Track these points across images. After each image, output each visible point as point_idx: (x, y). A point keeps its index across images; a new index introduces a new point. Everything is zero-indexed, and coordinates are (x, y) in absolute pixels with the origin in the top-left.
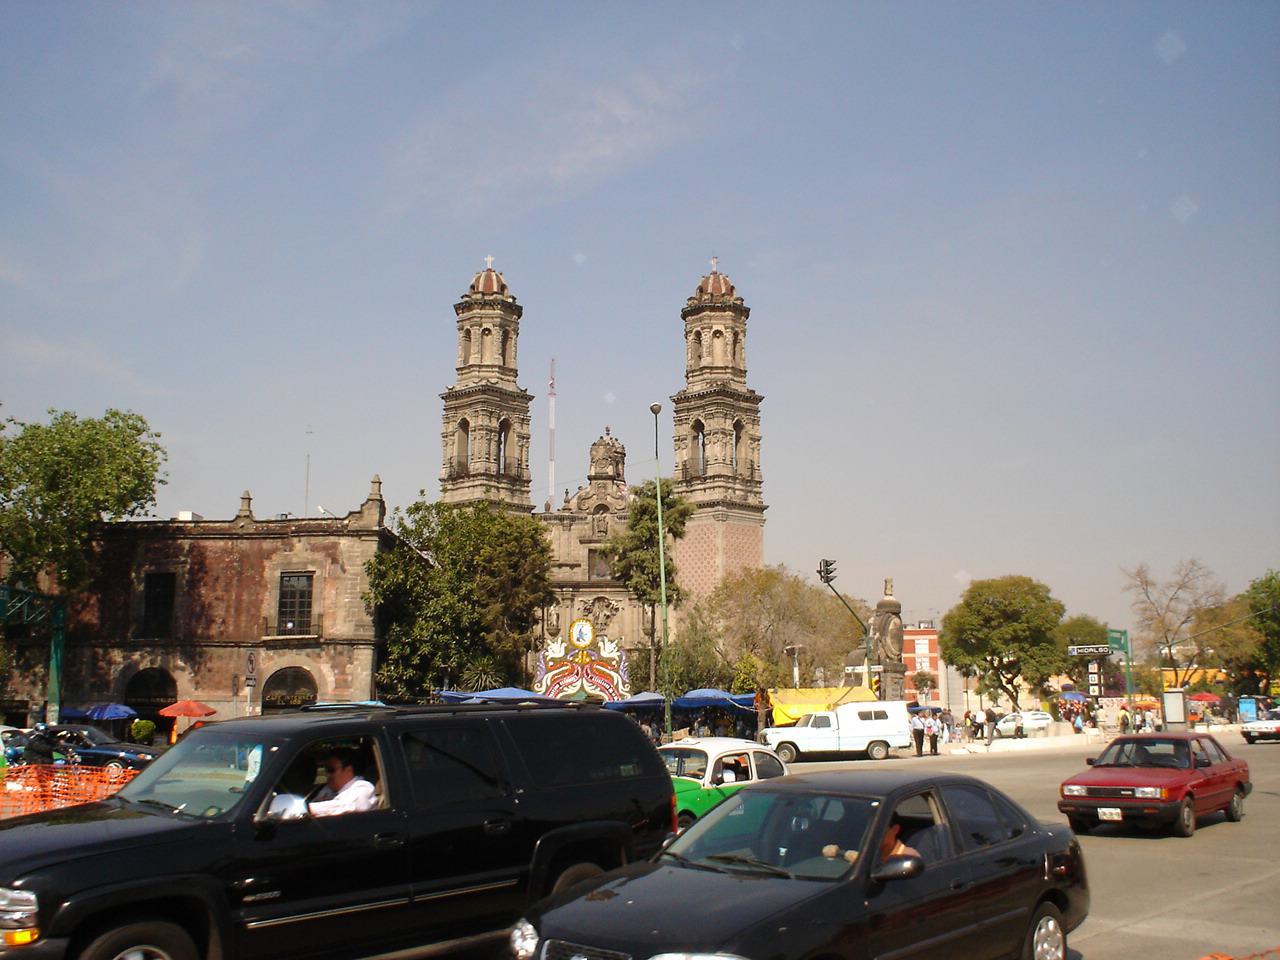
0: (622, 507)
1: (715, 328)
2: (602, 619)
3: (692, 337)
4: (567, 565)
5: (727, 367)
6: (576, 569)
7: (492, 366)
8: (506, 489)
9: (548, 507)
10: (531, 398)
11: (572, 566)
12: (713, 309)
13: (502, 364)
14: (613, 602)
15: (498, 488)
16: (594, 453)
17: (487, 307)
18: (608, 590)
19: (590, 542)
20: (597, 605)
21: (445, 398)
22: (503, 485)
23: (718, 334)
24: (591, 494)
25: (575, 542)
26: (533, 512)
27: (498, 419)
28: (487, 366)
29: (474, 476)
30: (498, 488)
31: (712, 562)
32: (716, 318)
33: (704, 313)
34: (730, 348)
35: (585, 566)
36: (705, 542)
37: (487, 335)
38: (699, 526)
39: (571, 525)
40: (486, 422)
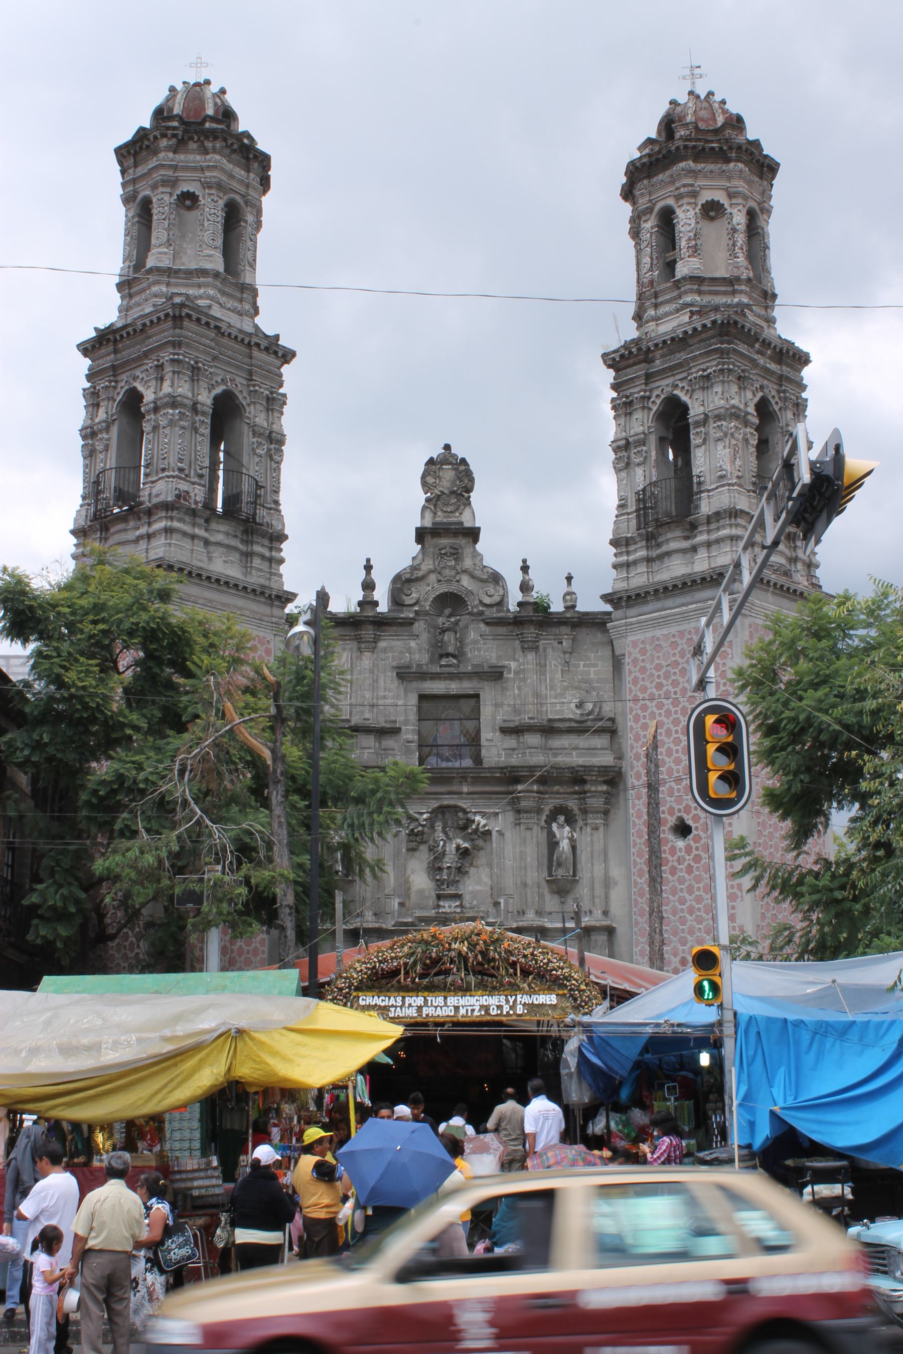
0: (496, 599)
1: (706, 196)
2: (450, 860)
3: (649, 225)
4: (367, 730)
5: (738, 279)
6: (389, 742)
7: (203, 272)
8: (228, 547)
9: (323, 597)
10: (287, 356)
11: (382, 733)
12: (699, 155)
13: (221, 268)
14: (478, 818)
15: (207, 543)
16: (430, 480)
17: (192, 145)
18: (465, 789)
19: (423, 676)
20: (439, 826)
21: (87, 349)
22: (220, 537)
23: (712, 211)
24: (425, 568)
25: (388, 682)
27: (210, 391)
28: (189, 273)
29: (149, 513)
30: (207, 543)
32: (710, 175)
33: (682, 165)
34: (741, 239)
35: (409, 733)
37: (189, 208)
38: (681, 633)
39: (376, 640)
40: (184, 389)
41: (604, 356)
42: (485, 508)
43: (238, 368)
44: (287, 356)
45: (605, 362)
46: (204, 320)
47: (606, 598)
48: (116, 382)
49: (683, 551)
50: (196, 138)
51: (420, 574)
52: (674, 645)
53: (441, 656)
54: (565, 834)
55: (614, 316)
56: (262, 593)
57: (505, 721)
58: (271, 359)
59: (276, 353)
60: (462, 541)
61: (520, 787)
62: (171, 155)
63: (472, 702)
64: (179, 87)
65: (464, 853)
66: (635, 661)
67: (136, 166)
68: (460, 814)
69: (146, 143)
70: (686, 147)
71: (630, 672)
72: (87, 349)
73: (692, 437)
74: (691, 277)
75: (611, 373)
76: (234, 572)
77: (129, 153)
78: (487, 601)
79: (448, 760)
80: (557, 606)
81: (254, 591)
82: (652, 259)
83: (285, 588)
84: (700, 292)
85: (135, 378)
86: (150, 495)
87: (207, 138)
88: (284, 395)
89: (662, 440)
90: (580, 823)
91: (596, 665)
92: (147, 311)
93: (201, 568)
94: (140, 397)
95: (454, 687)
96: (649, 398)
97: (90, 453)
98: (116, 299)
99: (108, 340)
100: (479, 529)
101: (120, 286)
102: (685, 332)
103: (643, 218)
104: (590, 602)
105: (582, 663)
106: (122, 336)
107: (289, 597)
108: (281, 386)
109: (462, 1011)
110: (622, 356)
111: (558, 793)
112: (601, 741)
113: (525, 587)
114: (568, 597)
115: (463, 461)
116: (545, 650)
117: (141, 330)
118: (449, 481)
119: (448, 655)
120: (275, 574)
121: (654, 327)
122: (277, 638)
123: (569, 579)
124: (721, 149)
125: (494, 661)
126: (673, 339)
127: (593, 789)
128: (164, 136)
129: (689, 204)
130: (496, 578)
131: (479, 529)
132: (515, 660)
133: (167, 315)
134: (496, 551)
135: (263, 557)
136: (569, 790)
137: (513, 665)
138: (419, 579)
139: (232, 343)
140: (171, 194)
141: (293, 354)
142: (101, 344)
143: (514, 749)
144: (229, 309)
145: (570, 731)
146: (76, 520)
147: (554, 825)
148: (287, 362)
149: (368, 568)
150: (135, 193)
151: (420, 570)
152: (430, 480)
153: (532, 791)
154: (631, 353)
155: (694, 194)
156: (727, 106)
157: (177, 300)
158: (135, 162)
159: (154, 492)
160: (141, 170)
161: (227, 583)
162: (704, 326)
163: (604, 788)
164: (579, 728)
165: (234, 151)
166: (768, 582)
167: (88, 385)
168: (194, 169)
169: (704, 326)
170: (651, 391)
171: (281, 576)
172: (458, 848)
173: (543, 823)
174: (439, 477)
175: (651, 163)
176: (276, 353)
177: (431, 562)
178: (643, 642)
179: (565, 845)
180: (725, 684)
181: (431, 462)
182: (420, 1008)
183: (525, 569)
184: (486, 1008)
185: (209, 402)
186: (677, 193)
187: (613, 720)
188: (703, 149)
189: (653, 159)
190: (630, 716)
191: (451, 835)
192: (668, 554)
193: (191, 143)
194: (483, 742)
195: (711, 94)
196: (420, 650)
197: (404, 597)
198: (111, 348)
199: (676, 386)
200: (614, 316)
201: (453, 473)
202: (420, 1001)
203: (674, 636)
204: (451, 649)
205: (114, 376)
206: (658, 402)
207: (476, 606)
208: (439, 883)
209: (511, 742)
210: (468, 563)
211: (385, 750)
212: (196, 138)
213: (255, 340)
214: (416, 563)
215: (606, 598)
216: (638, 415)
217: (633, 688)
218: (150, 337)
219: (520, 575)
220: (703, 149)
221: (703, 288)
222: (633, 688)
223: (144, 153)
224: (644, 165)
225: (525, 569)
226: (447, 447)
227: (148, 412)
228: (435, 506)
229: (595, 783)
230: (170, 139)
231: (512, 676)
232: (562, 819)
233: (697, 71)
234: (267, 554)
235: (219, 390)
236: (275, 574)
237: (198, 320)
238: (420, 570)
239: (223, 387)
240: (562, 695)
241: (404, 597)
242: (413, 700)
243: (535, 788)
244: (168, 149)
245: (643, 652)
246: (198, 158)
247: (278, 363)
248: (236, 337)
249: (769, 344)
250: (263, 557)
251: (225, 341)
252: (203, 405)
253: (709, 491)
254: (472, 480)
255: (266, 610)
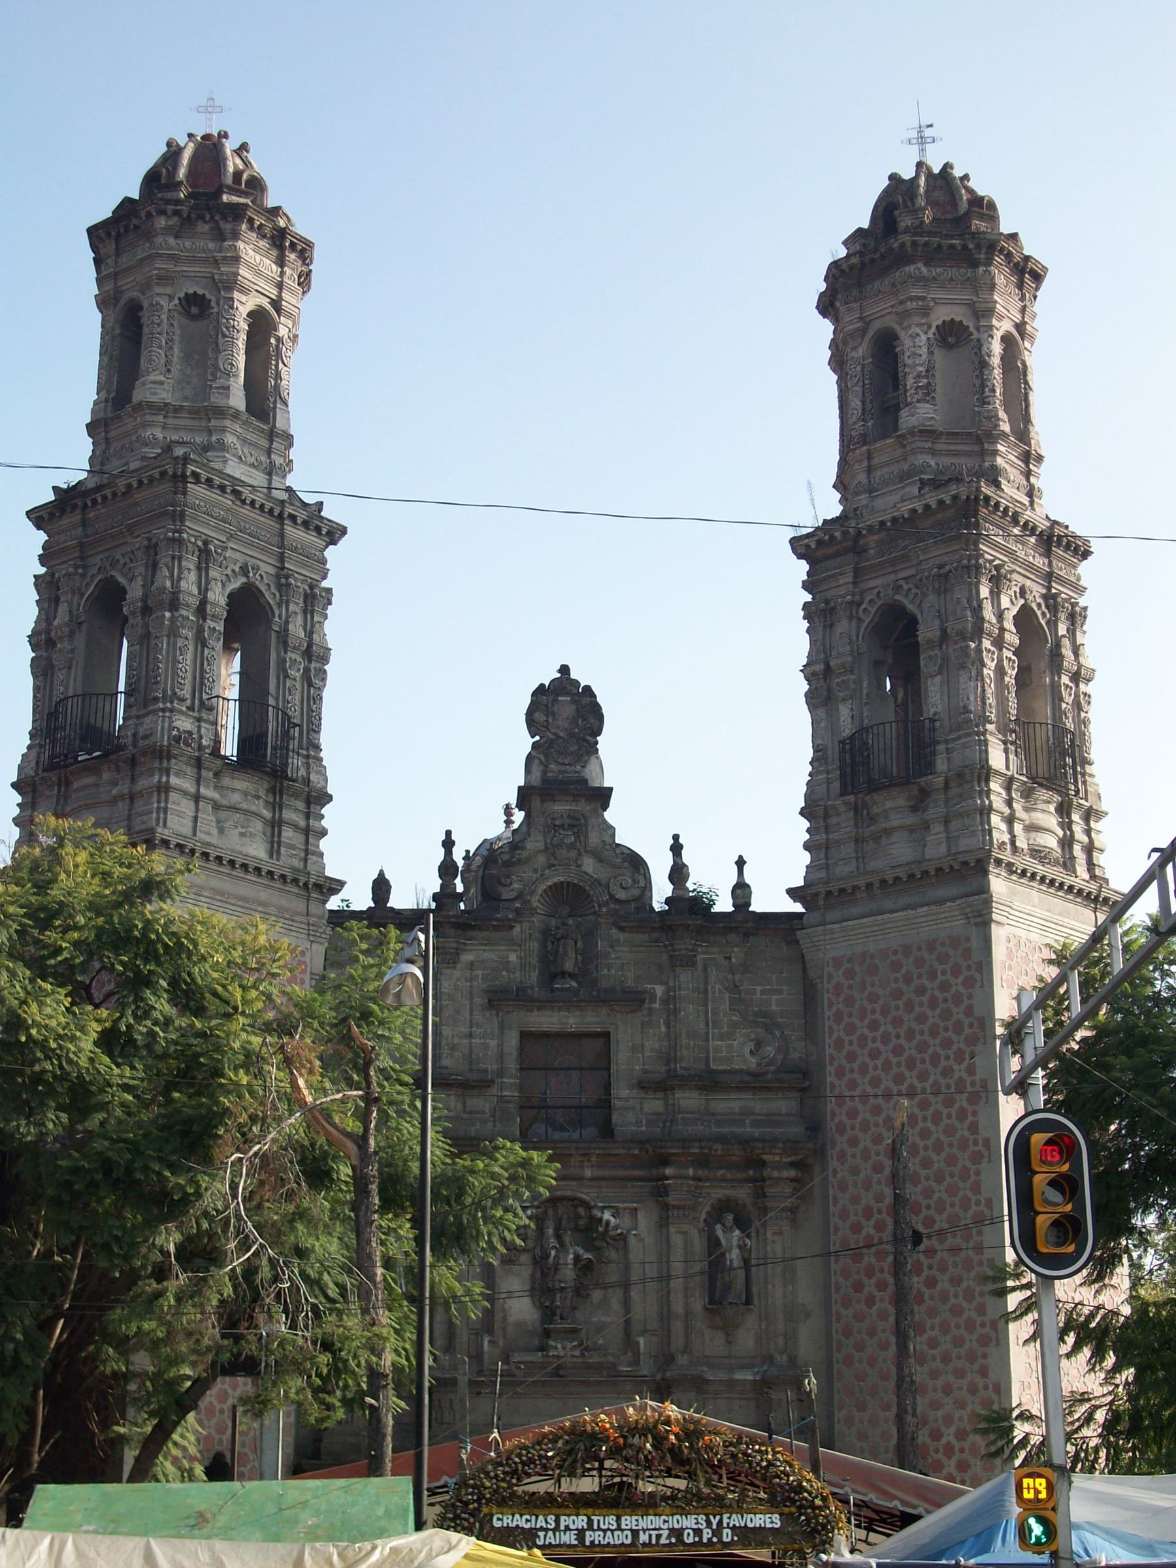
1: (942, 315)
3: (861, 352)
9: (381, 887)
10: (335, 533)
16: (539, 717)
21: (39, 517)
26: (334, 903)
27: (224, 586)
31: (959, 1071)
36: (933, 1003)
38: (907, 950)
41: (794, 542)
42: (617, 758)
43: (263, 550)
44: (335, 533)
45: (794, 551)
46: (217, 481)
47: (793, 893)
48: (85, 567)
49: (911, 830)
50: (208, 217)
51: (525, 854)
52: (896, 966)
53: (554, 977)
54: (735, 1242)
55: (809, 483)
56: (295, 881)
57: (647, 1072)
58: (310, 538)
59: (318, 529)
60: (583, 807)
61: (668, 1171)
62: (171, 241)
63: (600, 1042)
64: (182, 140)
65: (584, 1268)
66: (838, 989)
67: (118, 253)
68: (581, 1211)
69: (135, 221)
70: (914, 243)
71: (831, 1004)
72: (39, 517)
73: (922, 663)
74: (921, 431)
75: (803, 567)
76: (257, 850)
77: (109, 235)
78: (622, 895)
79: (562, 1129)
80: (724, 904)
81: (283, 877)
82: (863, 402)
83: (329, 873)
84: (932, 452)
85: (114, 563)
86: (135, 735)
87: (224, 218)
88: (329, 591)
89: (877, 664)
90: (757, 1224)
91: (779, 992)
92: (133, 466)
93: (208, 844)
94: (121, 592)
95: (572, 1021)
96: (859, 604)
97: (42, 670)
98: (86, 446)
99: (75, 506)
100: (611, 789)
101: (91, 428)
102: (914, 511)
103: (851, 344)
104: (772, 898)
105: (759, 988)
106: (95, 502)
107: (335, 886)
108: (324, 577)
109: (644, 1538)
110: (820, 543)
111: (724, 1180)
112: (784, 1105)
113: (678, 873)
114: (738, 891)
115: (588, 689)
116: (705, 969)
117: (124, 494)
118: (565, 718)
119: (563, 974)
120: (314, 853)
121: (865, 502)
122: (315, 946)
123: (741, 863)
124: (965, 247)
125: (630, 983)
126: (894, 520)
127: (776, 1174)
128: (162, 212)
129: (919, 325)
130: (636, 863)
131: (611, 789)
132: (661, 983)
133: (163, 474)
134: (635, 824)
135: (296, 827)
136: (740, 1176)
137: (659, 990)
138: (520, 862)
139: (255, 515)
140: (171, 298)
141: (343, 531)
142: (63, 512)
143: (658, 1114)
144: (252, 465)
145: (741, 1088)
146: (20, 768)
147: (718, 1227)
148: (334, 542)
149: (448, 843)
150: (118, 292)
151: (523, 849)
152: (539, 717)
153: (688, 1178)
154: (832, 537)
155: (925, 312)
156: (971, 184)
157: (179, 452)
158: (117, 249)
159: (141, 731)
160: (125, 261)
161: (245, 866)
162: (941, 502)
163: (792, 1173)
164: (753, 1083)
165: (264, 237)
166: (1033, 875)
167: (43, 570)
168: (205, 261)
169: (941, 502)
170: (862, 593)
171: (321, 855)
172: (577, 1259)
173: (701, 1225)
174: (553, 714)
175: (863, 264)
176: (318, 529)
177: (540, 838)
178: (850, 960)
179: (734, 1256)
180: (971, 1025)
181: (540, 691)
182: (581, 1533)
183: (676, 848)
184: (677, 1533)
185: (223, 601)
186: (900, 309)
187: (805, 1074)
188: (940, 246)
189: (867, 259)
190: (828, 1068)
191: (567, 1239)
192: (888, 832)
193: (200, 223)
194: (616, 1103)
195: (947, 167)
196: (523, 967)
197: (501, 889)
198: (77, 517)
199: (897, 589)
200: (809, 483)
201: (574, 707)
202: (581, 1522)
203: (896, 953)
204: (569, 966)
205: (82, 558)
206: (873, 610)
207: (606, 903)
208: (548, 1314)
209: (655, 1104)
210: (594, 839)
211: (471, 1112)
212: (208, 217)
213: (289, 510)
214: (517, 838)
215: (793, 893)
216: (843, 626)
217: (835, 1027)
218: (136, 504)
219: (669, 856)
220: (940, 246)
221: (938, 447)
222: (835, 1027)
223: (131, 236)
224: (852, 267)
225: (676, 848)
226: (564, 670)
227: (133, 613)
228: (546, 755)
229: (779, 1166)
230: (169, 217)
231: (657, 1006)
232: (729, 1218)
233: (928, 133)
234: (302, 823)
235: (235, 584)
236: (314, 853)
237: (209, 481)
238: (523, 849)
239: (244, 580)
240: (729, 1036)
241: (501, 889)
242: (512, 1041)
243: (691, 1171)
244: (168, 230)
245: (850, 974)
246: (211, 245)
247: (321, 543)
248: (262, 506)
249: (1034, 528)
250: (296, 827)
251: (245, 511)
252: (215, 605)
253: (947, 742)
254: (600, 718)
255: (299, 905)
